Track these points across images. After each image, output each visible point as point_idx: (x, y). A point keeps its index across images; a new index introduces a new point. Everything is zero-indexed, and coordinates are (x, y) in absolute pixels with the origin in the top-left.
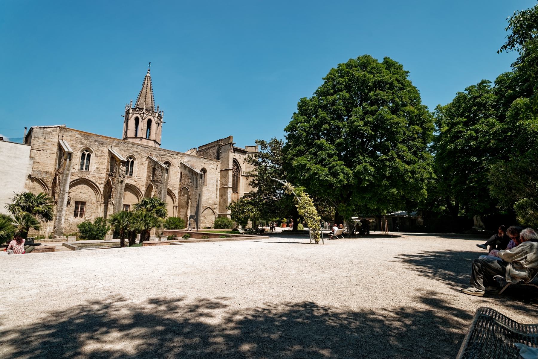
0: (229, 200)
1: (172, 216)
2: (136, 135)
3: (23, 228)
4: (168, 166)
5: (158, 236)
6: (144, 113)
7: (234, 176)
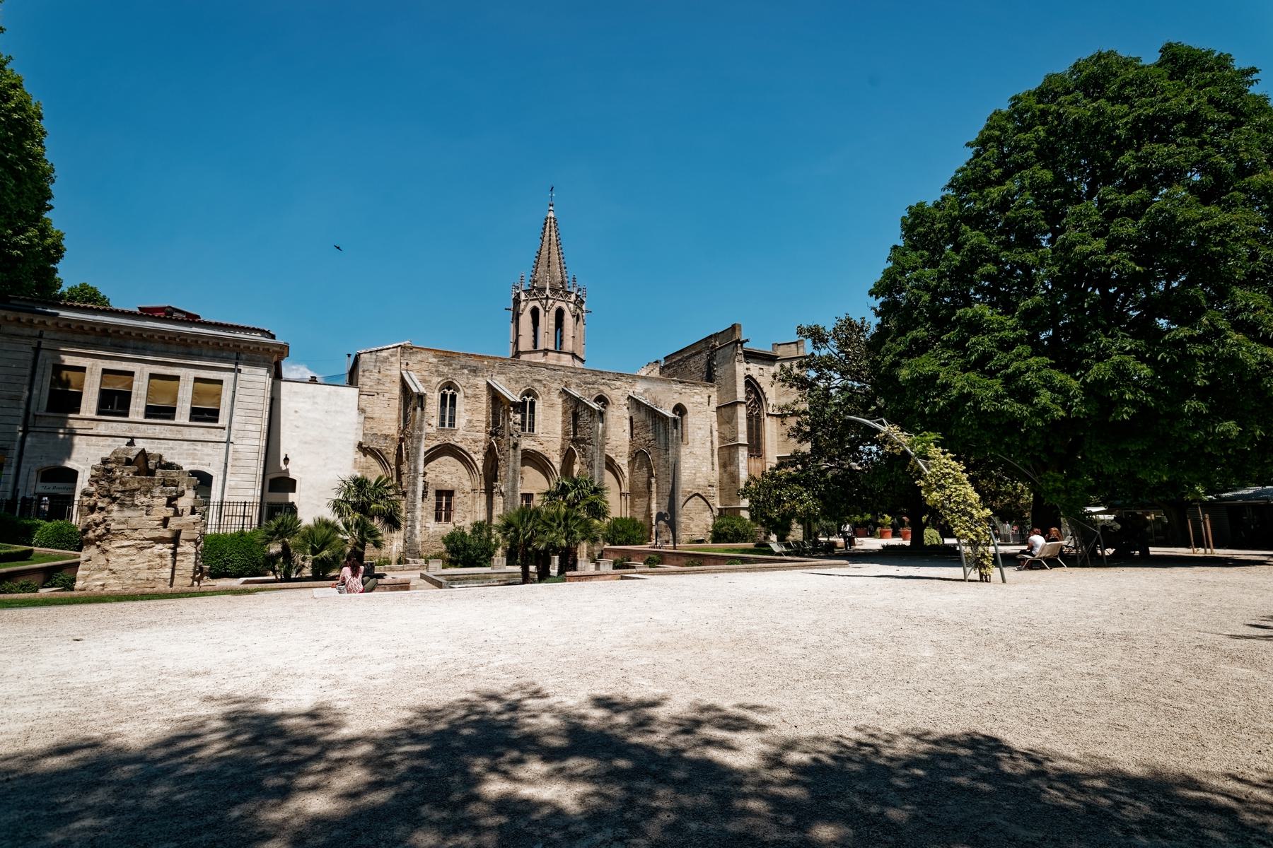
0: (743, 476)
1: (618, 516)
2: (535, 346)
3: (357, 544)
4: (603, 406)
5: (594, 561)
6: (547, 298)
7: (750, 418)
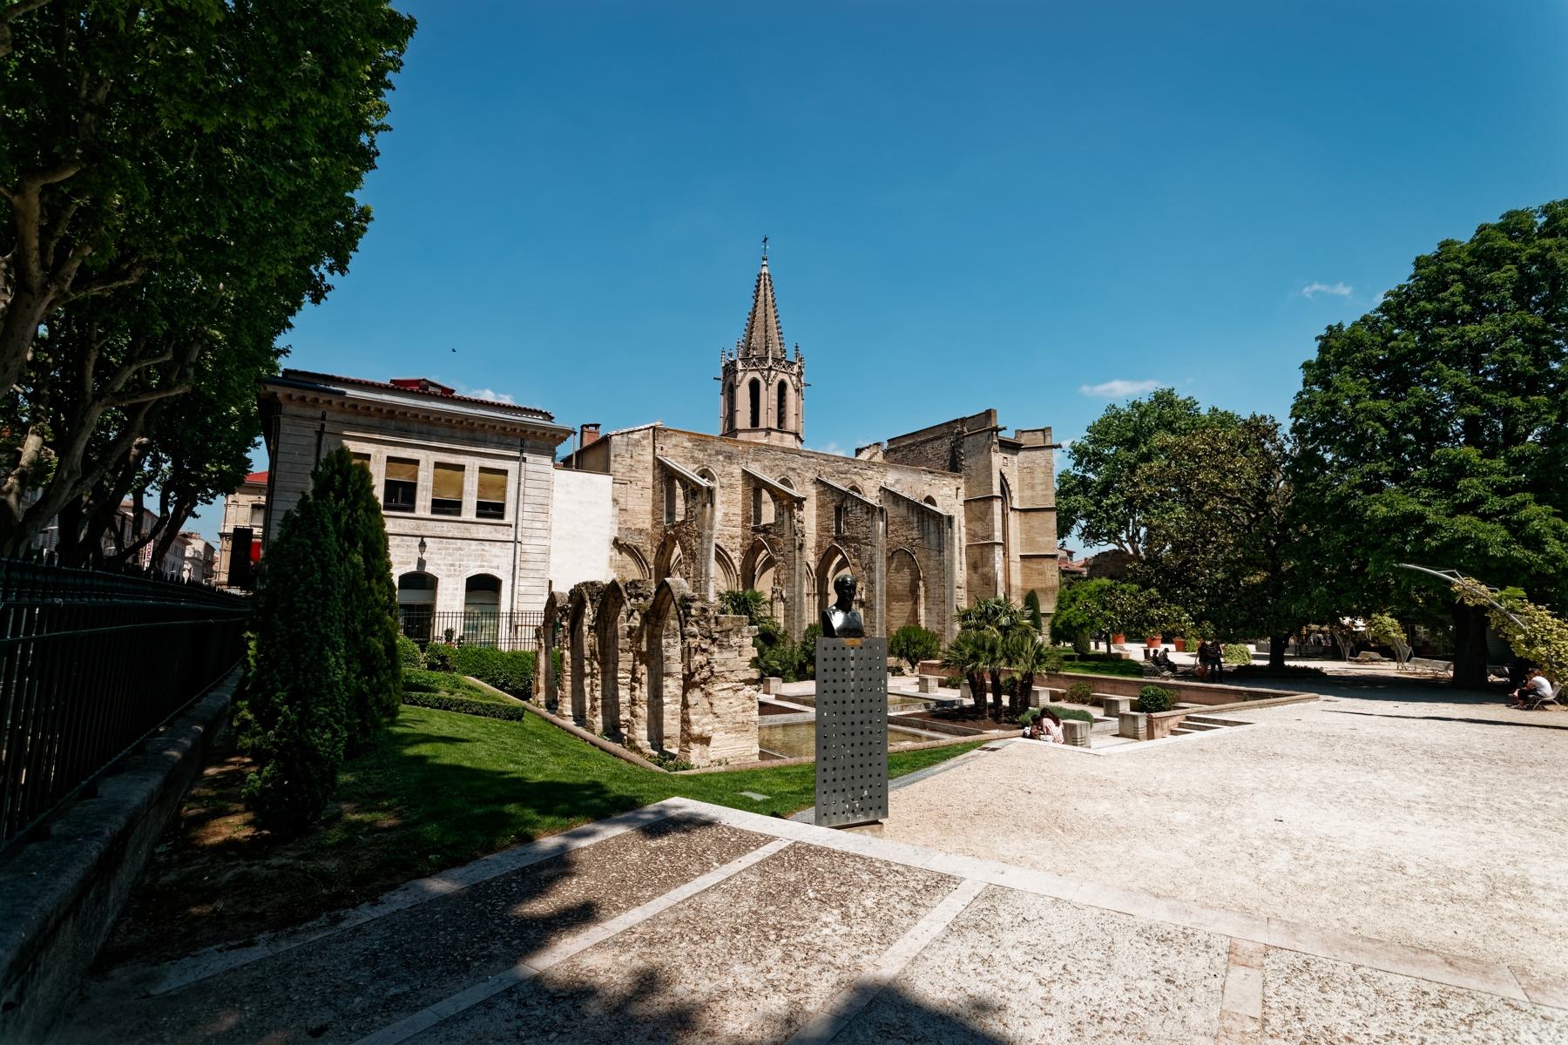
6: (770, 369)
